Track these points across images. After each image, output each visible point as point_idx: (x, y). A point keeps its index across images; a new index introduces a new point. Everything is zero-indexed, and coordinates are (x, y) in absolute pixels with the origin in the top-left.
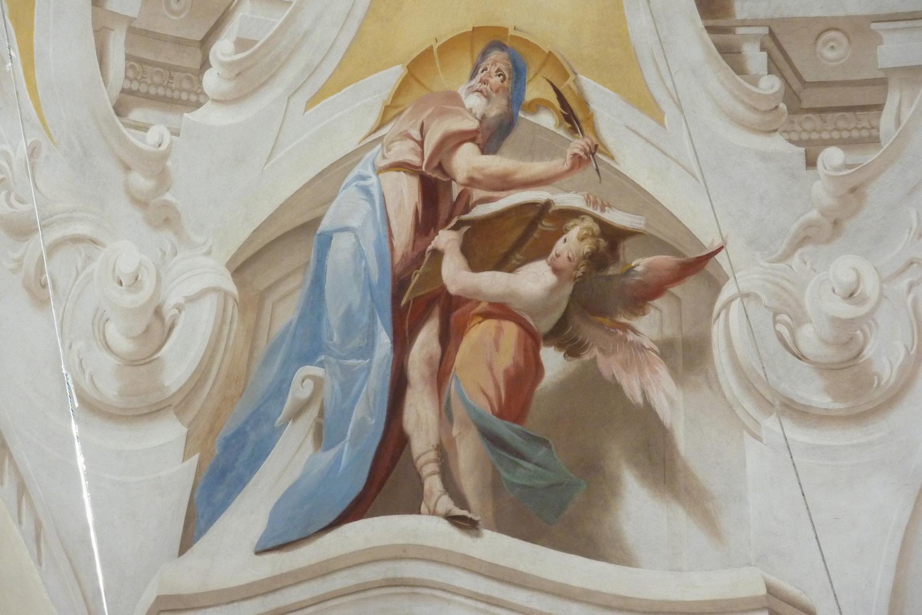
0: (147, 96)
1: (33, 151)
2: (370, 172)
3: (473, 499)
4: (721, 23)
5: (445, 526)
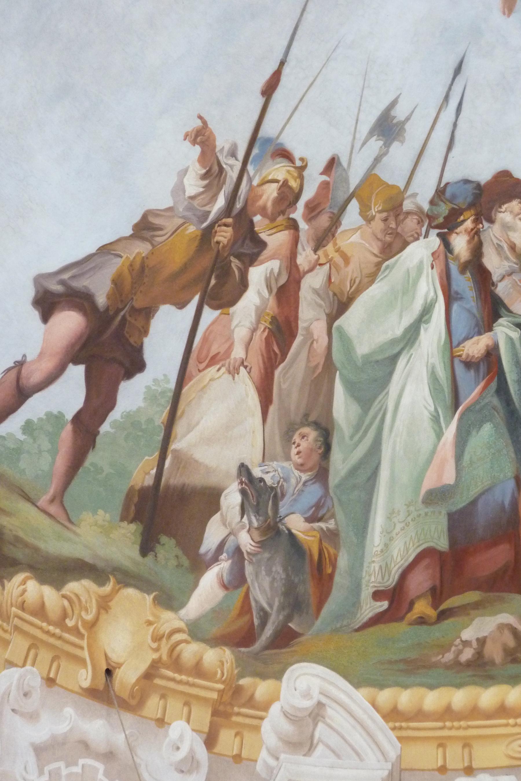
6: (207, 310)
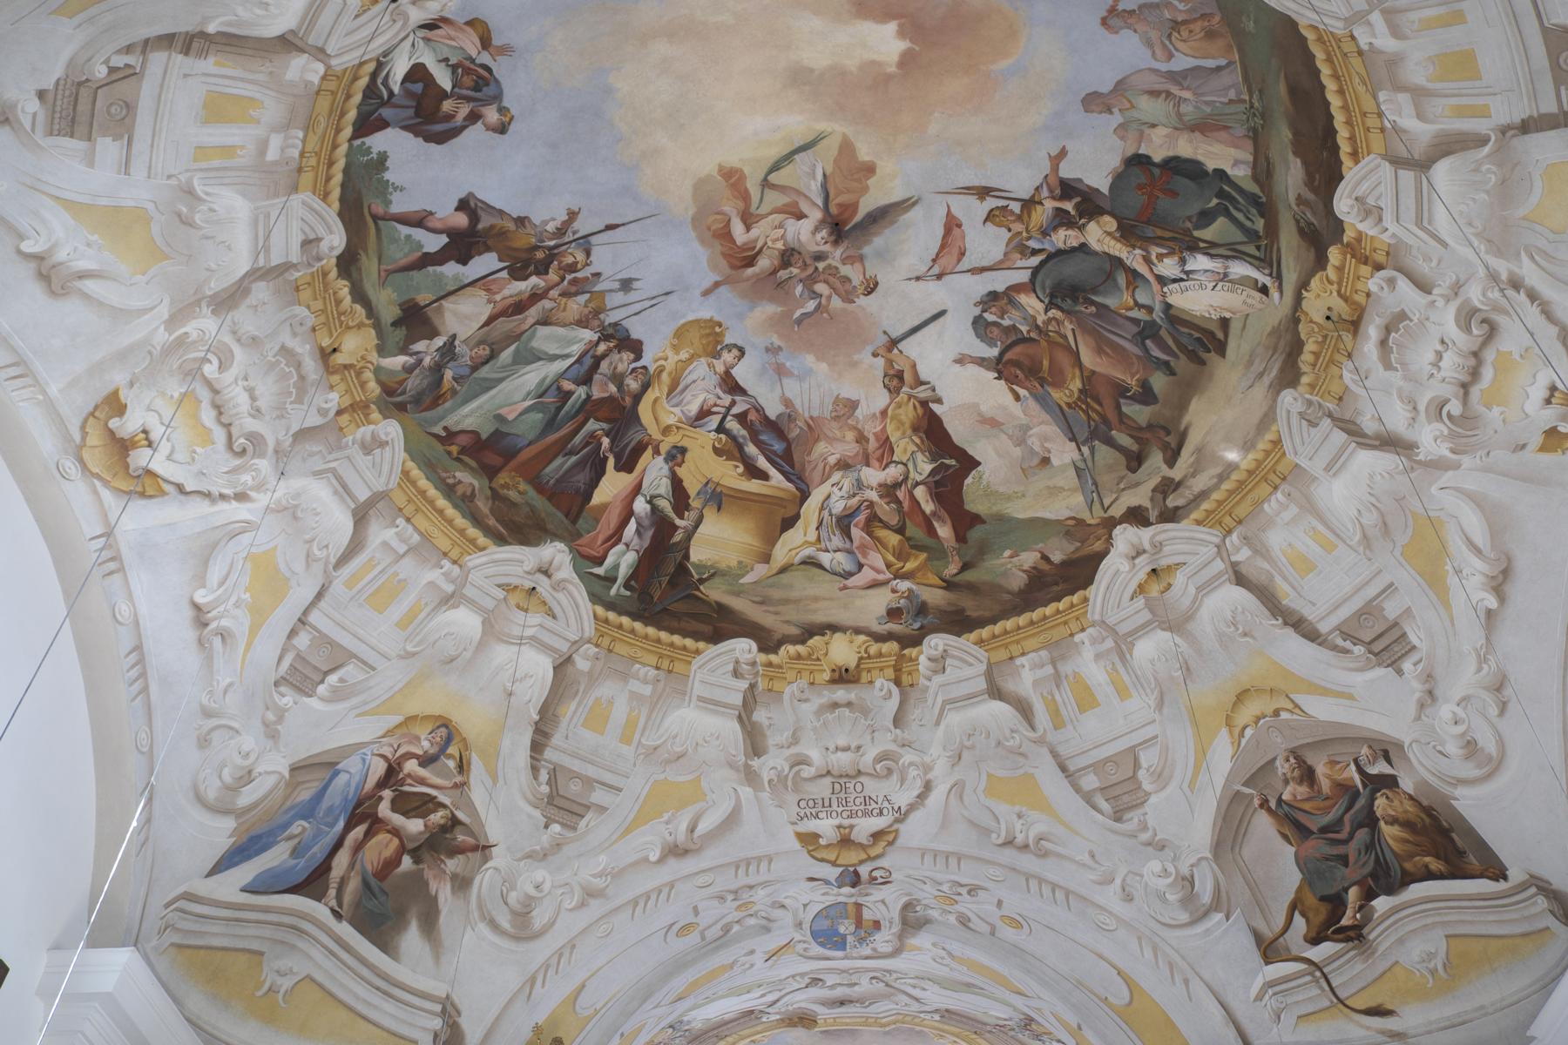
1: (231, 685)
2: (369, 753)
3: (345, 907)
5: (328, 912)
6: (505, 272)
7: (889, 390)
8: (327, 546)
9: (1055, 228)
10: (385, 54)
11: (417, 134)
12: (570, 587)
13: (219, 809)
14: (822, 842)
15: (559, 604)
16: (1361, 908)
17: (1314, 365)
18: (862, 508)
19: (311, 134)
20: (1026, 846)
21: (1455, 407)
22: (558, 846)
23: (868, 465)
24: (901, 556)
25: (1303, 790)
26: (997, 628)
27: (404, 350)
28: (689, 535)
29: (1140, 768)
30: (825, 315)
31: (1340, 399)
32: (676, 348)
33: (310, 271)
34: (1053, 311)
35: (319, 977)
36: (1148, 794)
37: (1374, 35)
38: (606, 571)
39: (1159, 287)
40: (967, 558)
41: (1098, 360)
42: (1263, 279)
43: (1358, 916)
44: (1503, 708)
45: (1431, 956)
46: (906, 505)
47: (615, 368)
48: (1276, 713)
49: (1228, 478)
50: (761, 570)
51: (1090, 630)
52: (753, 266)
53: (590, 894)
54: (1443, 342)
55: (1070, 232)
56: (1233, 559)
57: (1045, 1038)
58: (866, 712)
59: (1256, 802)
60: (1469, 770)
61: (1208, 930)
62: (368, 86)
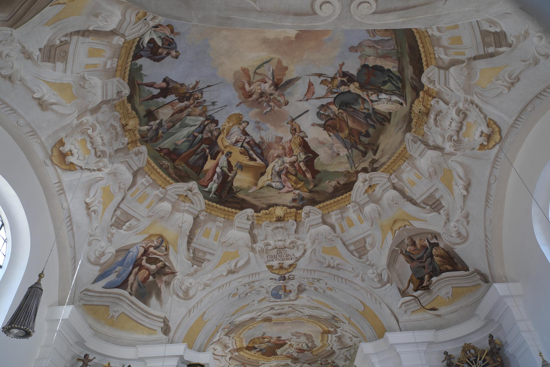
0: (115, 226)
1: (97, 227)
2: (139, 246)
3: (133, 292)
4: (189, 245)
5: (128, 293)
7: (292, 134)
8: (125, 184)
9: (341, 86)
10: (142, 35)
11: (151, 59)
12: (198, 195)
13: (95, 264)
14: (274, 268)
15: (194, 199)
16: (428, 281)
17: (416, 126)
18: (284, 169)
19: (120, 59)
20: (333, 267)
21: (455, 138)
22: (196, 272)
23: (286, 156)
24: (296, 183)
25: (412, 248)
26: (325, 204)
27: (147, 124)
28: (233, 178)
29: (366, 243)
30: (273, 112)
31: (423, 135)
32: (228, 122)
33: (119, 101)
34: (340, 110)
35: (126, 312)
36: (369, 251)
37: (433, 31)
38: (208, 190)
39: (371, 103)
40: (316, 183)
41: (354, 124)
42: (401, 101)
43: (428, 283)
44: (468, 222)
45: (448, 293)
46: (297, 168)
47: (210, 128)
48: (405, 226)
49: (391, 158)
50: (254, 188)
51: (352, 204)
52: (251, 97)
53: (206, 285)
54: (452, 119)
55: (345, 87)
56: (393, 182)
57: (338, 322)
58: (286, 229)
59: (399, 252)
60: (459, 241)
61: (386, 289)
62: (137, 45)
